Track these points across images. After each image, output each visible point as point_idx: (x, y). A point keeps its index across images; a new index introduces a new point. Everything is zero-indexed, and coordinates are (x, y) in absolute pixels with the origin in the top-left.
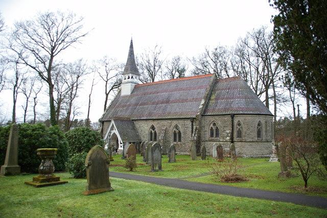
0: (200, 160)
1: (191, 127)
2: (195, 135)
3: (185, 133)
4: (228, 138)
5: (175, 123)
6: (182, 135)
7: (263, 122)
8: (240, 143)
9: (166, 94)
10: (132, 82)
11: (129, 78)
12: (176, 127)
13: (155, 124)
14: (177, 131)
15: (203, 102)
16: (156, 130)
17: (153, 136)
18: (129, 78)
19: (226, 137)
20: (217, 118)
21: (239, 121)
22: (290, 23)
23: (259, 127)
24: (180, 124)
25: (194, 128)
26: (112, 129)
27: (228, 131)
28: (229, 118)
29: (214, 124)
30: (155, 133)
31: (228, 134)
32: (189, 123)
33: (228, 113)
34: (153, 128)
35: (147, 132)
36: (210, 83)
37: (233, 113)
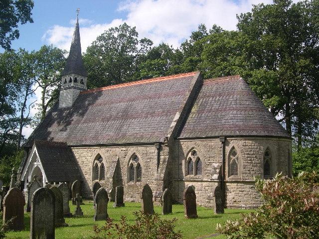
0: (123, 214)
1: (156, 157)
2: (162, 170)
3: (148, 167)
4: (216, 176)
5: (132, 150)
6: (143, 171)
7: (274, 148)
8: (235, 184)
9: (123, 105)
10: (75, 88)
11: (70, 81)
12: (134, 157)
13: (102, 151)
14: (135, 164)
15: (177, 116)
16: (104, 162)
17: (99, 172)
18: (70, 81)
19: (212, 175)
20: (198, 142)
21: (233, 148)
22: (5, 88)
23: (267, 158)
24: (139, 151)
25: (161, 160)
26: (34, 160)
27: (216, 165)
28: (218, 143)
29: (194, 153)
30: (102, 166)
31: (215, 169)
32: (153, 150)
33: (217, 135)
34: (99, 157)
35: (91, 165)
36: (191, 88)
37: (225, 133)
